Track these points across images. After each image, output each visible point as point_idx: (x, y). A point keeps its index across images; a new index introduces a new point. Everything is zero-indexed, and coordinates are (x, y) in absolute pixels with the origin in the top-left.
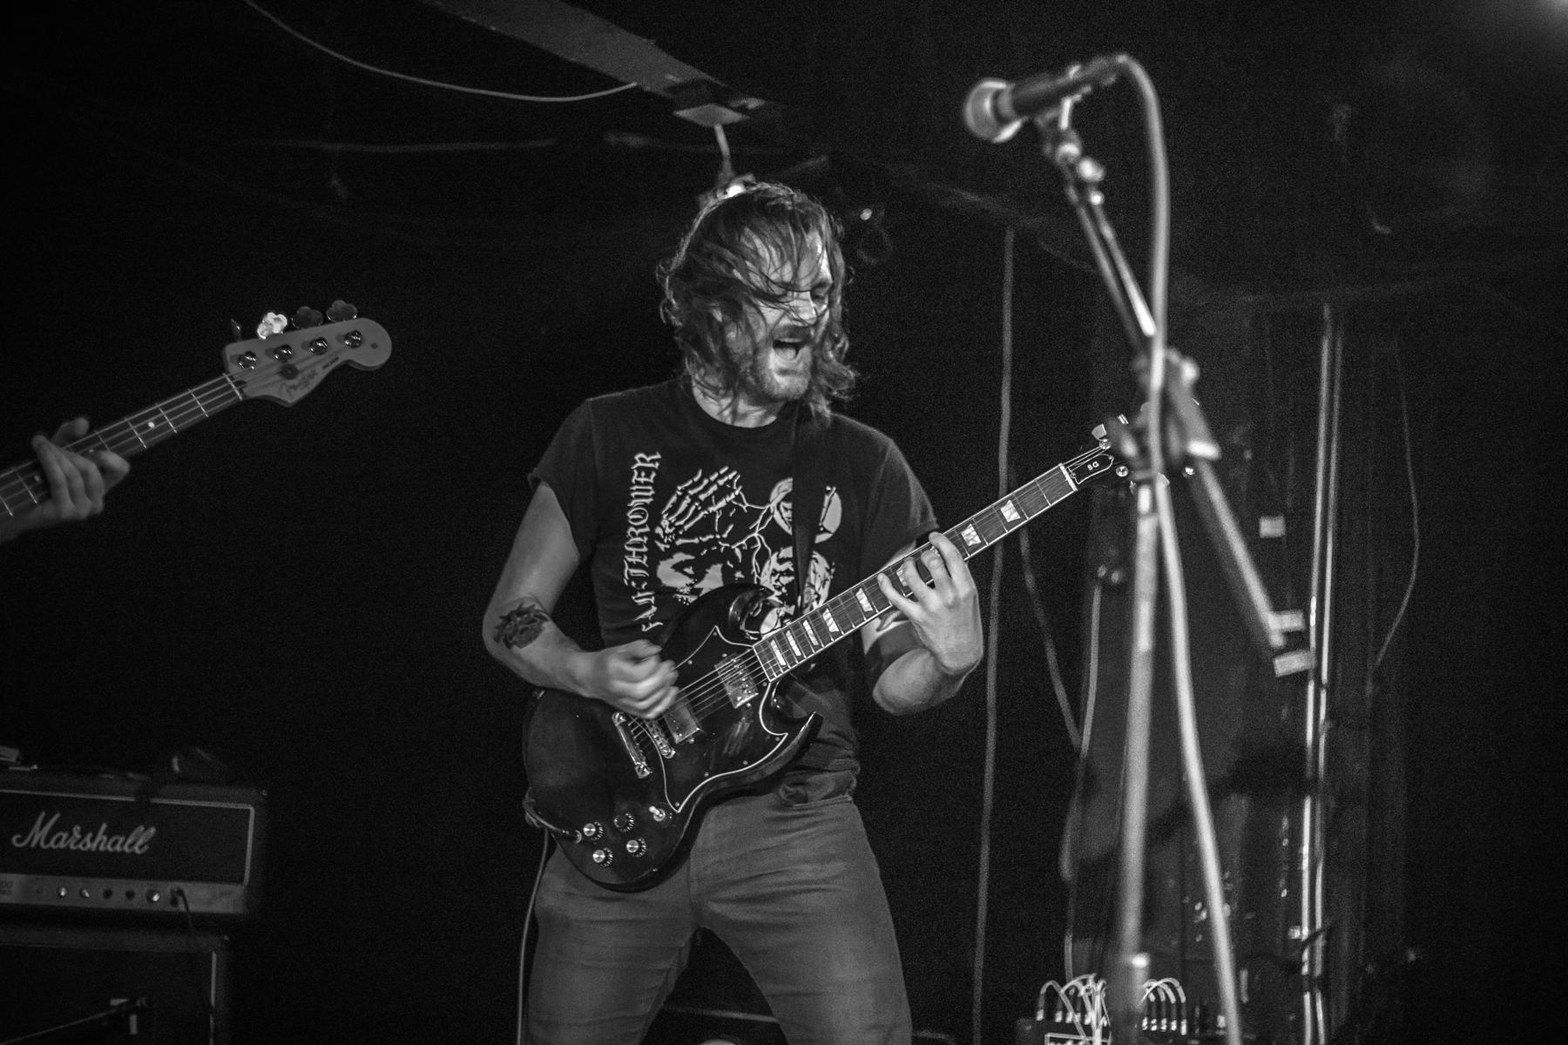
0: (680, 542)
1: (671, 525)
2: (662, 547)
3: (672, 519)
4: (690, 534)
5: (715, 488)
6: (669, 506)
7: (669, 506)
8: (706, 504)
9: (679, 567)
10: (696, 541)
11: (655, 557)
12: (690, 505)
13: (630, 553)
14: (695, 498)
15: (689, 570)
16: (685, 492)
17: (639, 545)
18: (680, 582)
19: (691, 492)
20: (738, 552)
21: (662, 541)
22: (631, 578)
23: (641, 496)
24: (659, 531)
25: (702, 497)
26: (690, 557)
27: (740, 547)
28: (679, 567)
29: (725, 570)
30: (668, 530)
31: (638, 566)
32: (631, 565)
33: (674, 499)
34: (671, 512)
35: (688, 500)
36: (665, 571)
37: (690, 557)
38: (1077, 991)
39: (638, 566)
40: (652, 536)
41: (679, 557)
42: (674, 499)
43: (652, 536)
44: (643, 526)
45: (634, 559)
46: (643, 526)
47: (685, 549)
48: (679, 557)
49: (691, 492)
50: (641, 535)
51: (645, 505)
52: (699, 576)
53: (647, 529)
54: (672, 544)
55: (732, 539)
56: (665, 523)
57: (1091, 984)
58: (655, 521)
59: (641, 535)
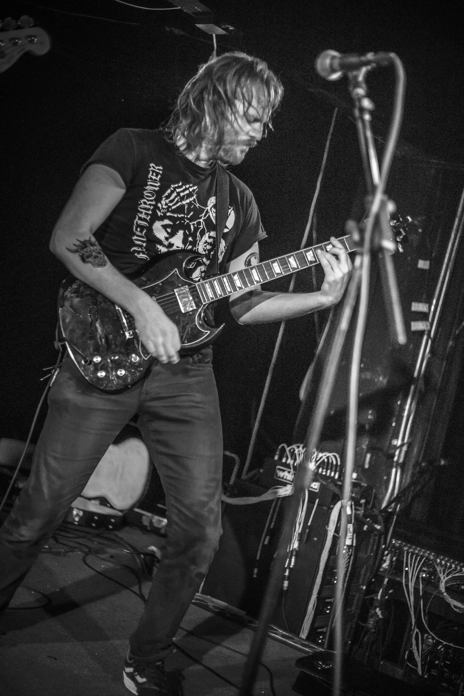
0: (168, 214)
1: (166, 204)
2: (159, 214)
3: (167, 201)
4: (173, 211)
5: (187, 192)
6: (166, 194)
7: (166, 194)
8: (182, 199)
9: (165, 227)
10: (176, 216)
11: (154, 218)
12: (176, 197)
13: (142, 213)
14: (178, 194)
15: (169, 230)
16: (175, 189)
17: (148, 210)
18: (161, 234)
19: (178, 190)
20: (192, 227)
21: (160, 211)
22: (138, 226)
23: (152, 186)
24: (159, 205)
25: (182, 194)
26: (171, 223)
27: (194, 224)
28: (165, 227)
29: (185, 234)
30: (164, 207)
31: (144, 220)
32: (140, 219)
33: (169, 191)
34: (167, 197)
35: (174, 194)
36: (157, 225)
37: (171, 223)
38: (294, 450)
39: (144, 220)
40: (156, 207)
41: (167, 222)
42: (169, 191)
43: (156, 207)
44: (152, 201)
45: (143, 216)
46: (152, 201)
47: (170, 218)
48: (167, 222)
49: (178, 190)
50: (150, 205)
51: (154, 191)
52: (172, 235)
53: (154, 203)
54: (165, 214)
55: (191, 219)
56: (163, 202)
57: (301, 448)
58: (158, 200)
59: (150, 205)
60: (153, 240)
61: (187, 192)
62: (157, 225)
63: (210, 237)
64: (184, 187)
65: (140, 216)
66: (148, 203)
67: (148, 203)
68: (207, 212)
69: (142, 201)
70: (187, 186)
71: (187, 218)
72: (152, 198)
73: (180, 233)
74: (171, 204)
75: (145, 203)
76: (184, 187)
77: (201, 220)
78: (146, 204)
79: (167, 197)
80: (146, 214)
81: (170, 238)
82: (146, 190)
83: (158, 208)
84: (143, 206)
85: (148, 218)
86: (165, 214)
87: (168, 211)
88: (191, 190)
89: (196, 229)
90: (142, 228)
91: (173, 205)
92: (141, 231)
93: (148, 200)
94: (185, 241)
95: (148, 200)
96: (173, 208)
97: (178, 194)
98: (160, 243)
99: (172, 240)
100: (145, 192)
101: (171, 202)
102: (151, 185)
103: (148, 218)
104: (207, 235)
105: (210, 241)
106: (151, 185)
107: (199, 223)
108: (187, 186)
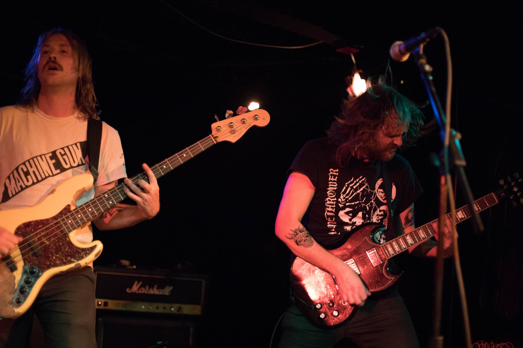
0: (347, 204)
1: (344, 198)
2: (341, 206)
3: (345, 195)
4: (350, 201)
5: (358, 184)
6: (343, 191)
7: (343, 191)
8: (356, 190)
9: (347, 213)
10: (353, 203)
11: (338, 209)
12: (350, 190)
13: (329, 207)
14: (352, 188)
15: (351, 215)
16: (348, 185)
17: (333, 205)
18: (346, 219)
19: (351, 185)
20: (368, 208)
21: (341, 204)
22: (328, 216)
23: (332, 188)
24: (340, 200)
25: (355, 187)
26: (351, 209)
27: (368, 206)
28: (347, 213)
29: (363, 214)
30: (343, 200)
31: (331, 212)
32: (328, 211)
33: (344, 188)
34: (344, 193)
35: (349, 189)
36: (341, 213)
37: (351, 209)
38: (478, 346)
39: (331, 212)
40: (337, 202)
41: (348, 210)
42: (344, 188)
43: (337, 202)
44: (334, 198)
45: (330, 209)
46: (334, 198)
47: (349, 206)
48: (348, 210)
49: (351, 185)
50: (333, 201)
51: (334, 190)
52: (354, 216)
53: (335, 199)
54: (345, 205)
56: (342, 197)
57: (482, 344)
58: (338, 196)
59: (333, 201)
60: (341, 224)
61: (358, 184)
62: (341, 213)
63: (380, 211)
64: (355, 182)
65: (328, 209)
66: (332, 200)
67: (332, 200)
68: (375, 194)
69: (327, 199)
70: (357, 180)
72: (334, 196)
73: (360, 214)
74: (348, 197)
75: (329, 200)
76: (355, 182)
77: (372, 201)
78: (330, 201)
79: (344, 193)
80: (331, 207)
81: (353, 218)
82: (328, 190)
83: (339, 202)
84: (328, 202)
85: (334, 211)
86: (345, 205)
88: (360, 182)
89: (370, 208)
90: (331, 217)
91: (350, 197)
92: (332, 219)
93: (331, 198)
94: (364, 218)
95: (331, 198)
96: (350, 199)
97: (352, 188)
98: (347, 224)
99: (354, 220)
100: (328, 192)
101: (347, 195)
102: (331, 187)
103: (334, 211)
104: (378, 210)
105: (382, 213)
106: (331, 187)
107: (372, 204)
108: (357, 180)
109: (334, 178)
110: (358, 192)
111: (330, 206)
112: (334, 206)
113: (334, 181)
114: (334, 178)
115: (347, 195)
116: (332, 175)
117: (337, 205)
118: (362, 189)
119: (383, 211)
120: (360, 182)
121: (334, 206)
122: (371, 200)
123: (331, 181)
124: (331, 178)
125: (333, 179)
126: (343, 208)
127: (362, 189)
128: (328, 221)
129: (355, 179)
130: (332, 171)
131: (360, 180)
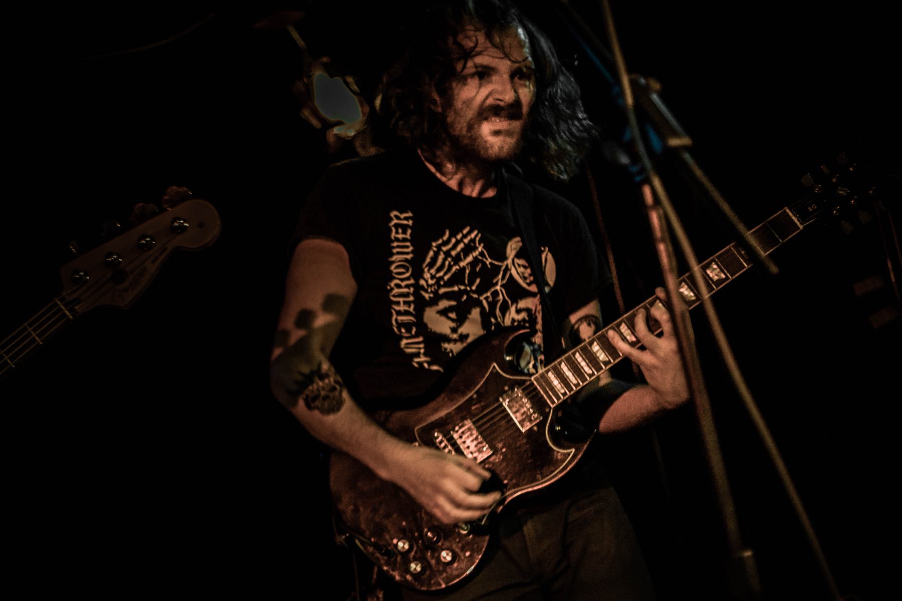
1: (432, 277)
2: (427, 296)
3: (433, 271)
5: (461, 246)
6: (428, 260)
7: (428, 260)
8: (457, 259)
11: (421, 305)
12: (445, 260)
13: (398, 303)
14: (447, 254)
16: (439, 247)
19: (444, 249)
21: (426, 291)
24: (422, 282)
25: (453, 253)
30: (430, 282)
31: (406, 313)
32: (399, 313)
33: (431, 254)
34: (431, 265)
35: (441, 257)
39: (406, 313)
40: (418, 288)
42: (431, 254)
43: (418, 288)
44: (408, 279)
45: (402, 308)
46: (408, 279)
50: (407, 286)
51: (406, 260)
53: (412, 281)
54: (436, 293)
56: (427, 275)
58: (418, 274)
61: (461, 246)
64: (453, 240)
71: (474, 292)
76: (453, 240)
77: (498, 288)
80: (405, 303)
84: (396, 291)
87: (440, 287)
88: (466, 241)
90: (408, 326)
91: (445, 274)
96: (446, 278)
97: (447, 254)
102: (398, 253)
105: (523, 315)
106: (398, 253)
108: (459, 236)
109: (404, 232)
110: (462, 264)
111: (401, 300)
112: (411, 298)
113: (405, 240)
114: (404, 232)
115: (438, 270)
116: (396, 226)
117: (417, 294)
118: (470, 259)
119: (528, 310)
120: (466, 241)
121: (411, 298)
122: (496, 283)
123: (397, 240)
124: (397, 233)
125: (400, 236)
126: (434, 302)
127: (470, 259)
128: (401, 338)
129: (453, 234)
130: (397, 218)
131: (465, 236)
